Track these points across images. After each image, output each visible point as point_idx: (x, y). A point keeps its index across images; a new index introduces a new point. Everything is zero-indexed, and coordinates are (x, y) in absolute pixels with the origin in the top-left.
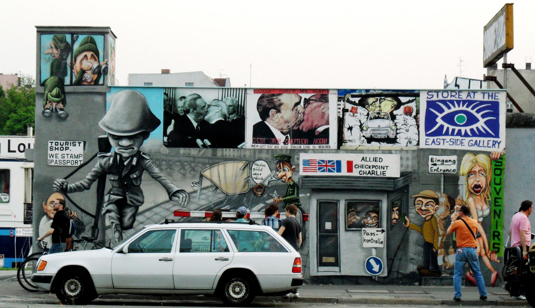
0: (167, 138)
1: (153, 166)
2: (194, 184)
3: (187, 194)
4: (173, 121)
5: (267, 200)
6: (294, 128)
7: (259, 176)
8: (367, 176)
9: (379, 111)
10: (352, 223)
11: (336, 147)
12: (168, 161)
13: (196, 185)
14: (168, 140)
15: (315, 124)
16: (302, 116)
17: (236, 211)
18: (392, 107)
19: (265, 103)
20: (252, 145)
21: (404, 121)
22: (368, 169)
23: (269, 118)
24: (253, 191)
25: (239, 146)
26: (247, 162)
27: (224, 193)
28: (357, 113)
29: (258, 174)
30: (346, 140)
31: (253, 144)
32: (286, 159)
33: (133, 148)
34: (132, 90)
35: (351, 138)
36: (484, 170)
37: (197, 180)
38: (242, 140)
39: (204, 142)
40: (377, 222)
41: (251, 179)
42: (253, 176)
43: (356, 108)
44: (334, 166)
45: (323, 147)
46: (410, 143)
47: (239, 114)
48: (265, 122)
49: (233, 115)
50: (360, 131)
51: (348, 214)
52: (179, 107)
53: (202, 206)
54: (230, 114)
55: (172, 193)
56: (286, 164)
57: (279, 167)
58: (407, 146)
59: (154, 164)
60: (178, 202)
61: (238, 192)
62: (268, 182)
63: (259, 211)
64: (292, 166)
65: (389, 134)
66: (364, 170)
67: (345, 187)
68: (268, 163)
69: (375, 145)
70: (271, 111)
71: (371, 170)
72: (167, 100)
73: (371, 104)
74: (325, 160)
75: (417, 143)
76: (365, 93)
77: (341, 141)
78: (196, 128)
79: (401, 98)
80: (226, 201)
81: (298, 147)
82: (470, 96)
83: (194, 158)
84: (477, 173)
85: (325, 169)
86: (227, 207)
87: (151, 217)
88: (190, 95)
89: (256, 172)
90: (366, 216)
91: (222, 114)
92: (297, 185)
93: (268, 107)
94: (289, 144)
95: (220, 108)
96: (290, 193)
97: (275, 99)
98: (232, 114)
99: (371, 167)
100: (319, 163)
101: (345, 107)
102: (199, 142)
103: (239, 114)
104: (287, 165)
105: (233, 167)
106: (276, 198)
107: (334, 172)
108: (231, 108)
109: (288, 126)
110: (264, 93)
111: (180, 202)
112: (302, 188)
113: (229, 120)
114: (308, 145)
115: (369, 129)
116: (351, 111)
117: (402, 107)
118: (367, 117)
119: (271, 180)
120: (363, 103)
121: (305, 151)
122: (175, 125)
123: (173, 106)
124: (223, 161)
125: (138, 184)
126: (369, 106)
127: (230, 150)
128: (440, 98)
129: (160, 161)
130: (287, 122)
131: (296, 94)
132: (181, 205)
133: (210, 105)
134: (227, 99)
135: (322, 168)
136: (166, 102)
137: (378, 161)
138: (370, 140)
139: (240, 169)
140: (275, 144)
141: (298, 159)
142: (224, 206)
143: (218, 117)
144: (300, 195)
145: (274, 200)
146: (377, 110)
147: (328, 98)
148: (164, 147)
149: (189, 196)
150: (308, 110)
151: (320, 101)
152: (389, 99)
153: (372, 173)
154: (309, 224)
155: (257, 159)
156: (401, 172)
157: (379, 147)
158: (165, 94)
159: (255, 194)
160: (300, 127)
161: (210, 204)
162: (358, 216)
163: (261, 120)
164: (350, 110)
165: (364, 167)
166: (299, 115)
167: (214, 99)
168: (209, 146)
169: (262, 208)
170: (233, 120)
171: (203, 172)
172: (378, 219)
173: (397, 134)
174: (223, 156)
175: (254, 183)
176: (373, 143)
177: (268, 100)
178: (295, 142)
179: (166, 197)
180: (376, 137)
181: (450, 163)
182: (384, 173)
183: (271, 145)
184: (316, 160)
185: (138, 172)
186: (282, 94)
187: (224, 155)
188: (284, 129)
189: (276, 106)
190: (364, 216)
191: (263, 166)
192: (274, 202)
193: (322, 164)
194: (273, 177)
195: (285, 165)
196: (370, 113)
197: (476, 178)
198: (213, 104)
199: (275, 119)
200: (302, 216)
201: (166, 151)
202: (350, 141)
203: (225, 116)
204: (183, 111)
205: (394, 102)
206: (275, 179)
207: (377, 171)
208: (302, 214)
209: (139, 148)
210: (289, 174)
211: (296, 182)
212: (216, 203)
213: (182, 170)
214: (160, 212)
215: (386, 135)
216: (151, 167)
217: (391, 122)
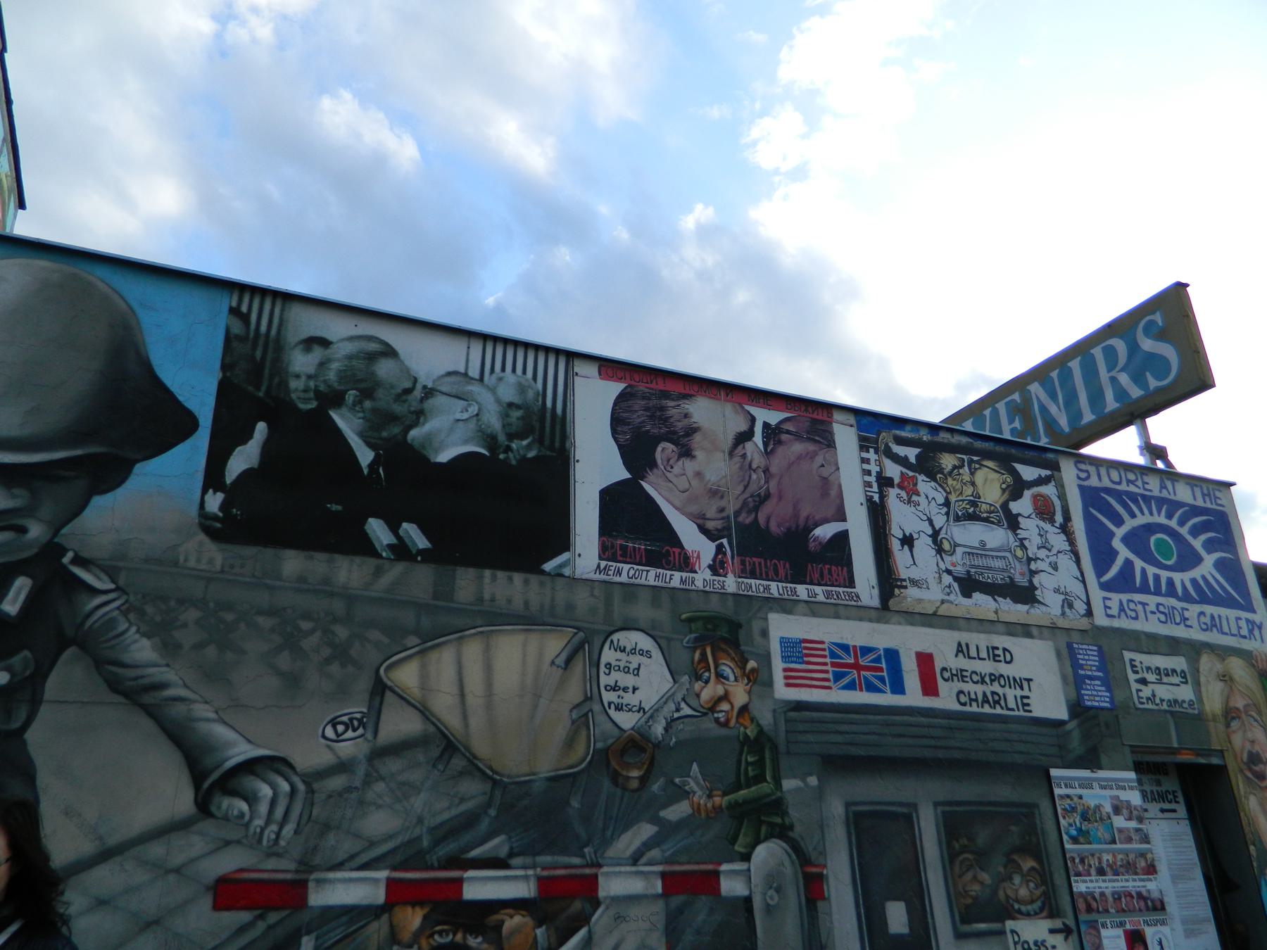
0: (220, 496)
1: (123, 626)
2: (340, 728)
3: (296, 779)
4: (261, 428)
5: (665, 806)
6: (740, 519)
7: (629, 698)
8: (980, 710)
9: (972, 495)
10: (969, 901)
11: (876, 602)
12: (212, 605)
13: (350, 734)
14: (223, 507)
15: (804, 514)
16: (763, 482)
17: (534, 867)
18: (1004, 490)
19: (638, 416)
20: (599, 566)
21: (1041, 536)
22: (979, 685)
23: (655, 470)
24: (608, 764)
25: (549, 566)
26: (581, 634)
27: (484, 773)
28: (918, 494)
29: (625, 689)
30: (903, 577)
31: (603, 564)
32: (723, 632)
33: (23, 530)
34: (67, 268)
35: (914, 573)
36: (1255, 705)
37: (357, 709)
38: (561, 540)
39: (401, 532)
40: (1044, 893)
41: (597, 708)
42: (608, 696)
43: (913, 476)
44: (881, 670)
45: (838, 594)
46: (1071, 606)
47: (547, 442)
48: (642, 482)
49: (525, 443)
50: (934, 552)
51: (952, 862)
52: (298, 376)
53: (372, 844)
54: (511, 436)
55: (215, 776)
56: (723, 651)
57: (700, 661)
58: (1063, 614)
59: (132, 616)
60: (247, 825)
61: (546, 766)
63: (635, 859)
64: (746, 661)
65: (1012, 571)
66: (969, 687)
67: (928, 753)
68: (659, 640)
69: (982, 604)
70: (659, 449)
71: (988, 689)
72: (242, 339)
73: (950, 473)
74: (851, 643)
75: (1085, 607)
76: (929, 438)
77: (888, 580)
78: (366, 471)
79: (1020, 468)
80: (493, 812)
81: (762, 589)
82: (1165, 488)
83: (350, 599)
84: (1243, 716)
85: (854, 680)
86: (497, 845)
88: (352, 339)
89: (616, 676)
90: (1005, 867)
91: (480, 430)
92: (770, 740)
93: (648, 431)
94: (730, 575)
95: (474, 409)
96: (751, 774)
97: (674, 409)
98: (521, 436)
99: (987, 679)
100: (833, 655)
101: (881, 469)
102: (378, 530)
103: (547, 442)
104: (729, 654)
105: (524, 655)
106: (699, 797)
107: (885, 692)
108: (516, 414)
109: (722, 510)
110: (633, 383)
111: (259, 822)
112: (788, 753)
113: (508, 458)
114: (794, 585)
115: (959, 550)
116: (901, 486)
117: (1027, 494)
118: (945, 509)
119: (676, 715)
120: (927, 466)
121: (786, 606)
122: (267, 449)
123: (268, 364)
124: (479, 622)
125: (16, 725)
126: (946, 479)
127: (510, 579)
128: (1106, 483)
129: (173, 603)
130: (715, 493)
131: (738, 407)
132: (260, 841)
133: (431, 389)
134: (500, 379)
135: (843, 675)
136: (235, 344)
137: (1002, 658)
138: (969, 585)
139: (553, 663)
140: (680, 570)
141: (765, 633)
143: (466, 442)
144: (788, 784)
146: (969, 491)
147: (831, 434)
148: (202, 537)
149: (311, 791)
150: (777, 464)
151: (809, 439)
152: (990, 464)
153: (998, 702)
154: (830, 914)
155: (619, 624)
156: (1067, 701)
157: (996, 612)
158: (234, 311)
159: (615, 778)
160: (759, 514)
161: (417, 831)
162: (982, 869)
163: (627, 475)
164: (897, 480)
165: (968, 679)
166: (754, 476)
167: (451, 369)
168: (422, 552)
169: (647, 846)
170: (524, 460)
172: (1044, 882)
173: (1033, 573)
174: (480, 600)
175: (609, 725)
176: (977, 596)
177: (647, 409)
178: (748, 568)
179: (183, 801)
180: (981, 579)
181: (1176, 680)
182: (1025, 701)
183: (669, 573)
184: (822, 643)
185: (26, 653)
186: (694, 396)
187: (487, 596)
188: (708, 516)
189: (675, 433)
190: (1001, 869)
191: (642, 653)
192: (692, 815)
193: (842, 658)
194: (683, 705)
195: (721, 654)
196: (953, 498)
197: (1245, 731)
198: (444, 389)
199: (676, 476)
200: (800, 876)
201: (211, 561)
202: (914, 583)
203: (490, 440)
204: (312, 395)
205: (1005, 476)
206: (690, 712)
207: (1004, 695)
208: (802, 866)
209: (57, 532)
210: (740, 695)
211: (766, 729)
212: (441, 824)
213: (286, 654)
215: (1006, 574)
216: (111, 634)
217: (1010, 533)
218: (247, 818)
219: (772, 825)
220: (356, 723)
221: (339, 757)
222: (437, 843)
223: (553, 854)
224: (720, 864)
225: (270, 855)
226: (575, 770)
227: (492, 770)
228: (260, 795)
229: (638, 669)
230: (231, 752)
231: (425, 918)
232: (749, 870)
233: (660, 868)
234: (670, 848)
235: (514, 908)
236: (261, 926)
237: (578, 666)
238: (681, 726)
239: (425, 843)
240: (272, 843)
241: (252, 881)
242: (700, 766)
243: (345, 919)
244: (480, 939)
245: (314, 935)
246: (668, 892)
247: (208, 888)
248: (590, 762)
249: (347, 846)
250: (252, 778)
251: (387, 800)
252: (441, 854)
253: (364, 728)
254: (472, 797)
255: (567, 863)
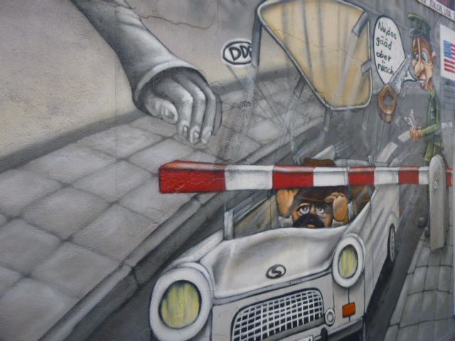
2: (235, 53)
7: (388, 64)
13: (241, 59)
24: (378, 105)
27: (321, 102)
29: (385, 57)
37: (245, 39)
41: (373, 67)
42: (379, 60)
53: (262, 146)
55: (146, 79)
56: (424, 42)
60: (177, 124)
61: (350, 101)
62: (401, 82)
63: (388, 164)
80: (326, 129)
86: (327, 152)
87: (37, 202)
106: (413, 129)
111: (185, 123)
119: (406, 79)
139: (353, 31)
141: (438, 36)
142: (322, 150)
144: (444, 125)
145: (410, 133)
149: (220, 102)
159: (382, 114)
161: (288, 139)
169: (393, 156)
171: (264, 9)
194: (408, 73)
195: (423, 45)
206: (411, 78)
212: (300, 135)
214: (87, 175)
218: (176, 118)
219: (438, 147)
220: (245, 51)
221: (236, 77)
222: (299, 147)
223: (355, 159)
224: (419, 167)
225: (196, 150)
226: (364, 106)
227: (325, 101)
228: (184, 100)
229: (390, 45)
230: (157, 59)
231: (295, 198)
232: (428, 171)
233: (397, 169)
234: (402, 157)
235: (339, 192)
236: (196, 205)
237: (365, 36)
238: (407, 86)
239: (292, 148)
240: (196, 141)
241: (185, 170)
242: (414, 112)
243: (250, 199)
244: (323, 211)
245: (232, 211)
246: (401, 182)
247: (154, 175)
248: (370, 102)
249: (247, 147)
250: (176, 84)
251: (269, 114)
252: (301, 155)
253: (251, 57)
254: (316, 118)
255: (359, 164)
